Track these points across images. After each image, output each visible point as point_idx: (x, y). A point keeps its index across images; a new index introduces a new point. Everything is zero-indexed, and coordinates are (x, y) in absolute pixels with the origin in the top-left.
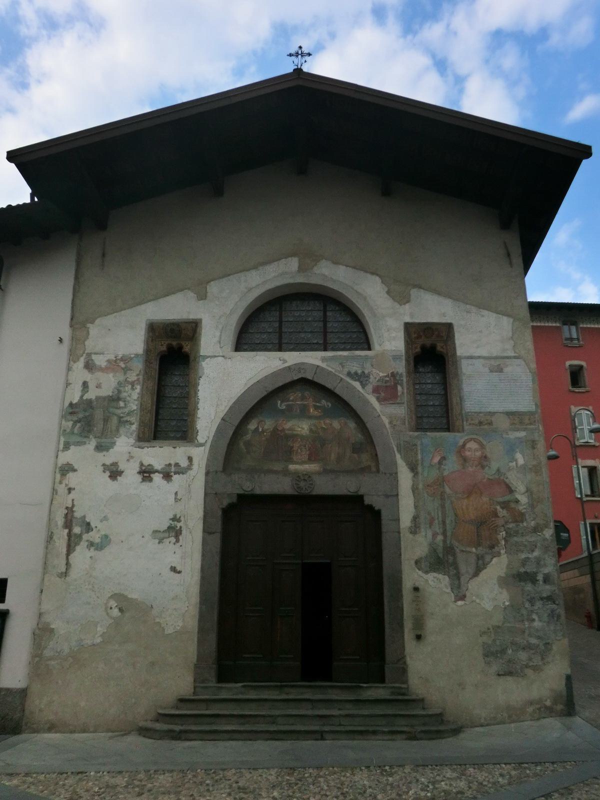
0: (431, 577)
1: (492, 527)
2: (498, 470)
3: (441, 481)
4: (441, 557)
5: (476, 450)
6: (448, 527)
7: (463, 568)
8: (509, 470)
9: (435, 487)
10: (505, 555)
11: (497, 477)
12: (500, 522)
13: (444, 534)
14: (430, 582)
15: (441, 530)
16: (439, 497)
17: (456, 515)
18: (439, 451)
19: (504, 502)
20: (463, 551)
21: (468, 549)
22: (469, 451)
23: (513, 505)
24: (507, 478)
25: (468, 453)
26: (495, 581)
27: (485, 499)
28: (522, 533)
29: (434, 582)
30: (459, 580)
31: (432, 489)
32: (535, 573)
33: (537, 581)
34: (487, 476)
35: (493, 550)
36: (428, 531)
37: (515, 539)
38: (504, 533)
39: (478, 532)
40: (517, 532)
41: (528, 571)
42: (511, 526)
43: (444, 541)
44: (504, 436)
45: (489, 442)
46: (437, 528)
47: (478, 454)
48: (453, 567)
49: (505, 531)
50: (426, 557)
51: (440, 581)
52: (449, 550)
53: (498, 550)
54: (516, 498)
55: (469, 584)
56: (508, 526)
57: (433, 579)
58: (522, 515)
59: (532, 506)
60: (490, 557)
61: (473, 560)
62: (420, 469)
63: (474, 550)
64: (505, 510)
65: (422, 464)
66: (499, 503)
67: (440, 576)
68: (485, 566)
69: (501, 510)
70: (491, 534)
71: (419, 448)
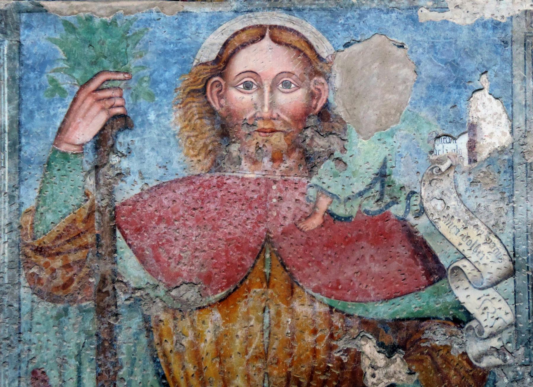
2: (382, 176)
3: (105, 225)
5: (282, 82)
8: (435, 171)
9: (72, 258)
11: (371, 206)
16: (89, 304)
19: (397, 324)
22: (248, 86)
23: (438, 336)
24: (422, 211)
25: (240, 99)
27: (309, 308)
31: (58, 263)
34: (324, 204)
45: (347, 45)
47: (292, 100)
54: (460, 306)
64: (398, 357)
66: (370, 326)
69: (381, 359)
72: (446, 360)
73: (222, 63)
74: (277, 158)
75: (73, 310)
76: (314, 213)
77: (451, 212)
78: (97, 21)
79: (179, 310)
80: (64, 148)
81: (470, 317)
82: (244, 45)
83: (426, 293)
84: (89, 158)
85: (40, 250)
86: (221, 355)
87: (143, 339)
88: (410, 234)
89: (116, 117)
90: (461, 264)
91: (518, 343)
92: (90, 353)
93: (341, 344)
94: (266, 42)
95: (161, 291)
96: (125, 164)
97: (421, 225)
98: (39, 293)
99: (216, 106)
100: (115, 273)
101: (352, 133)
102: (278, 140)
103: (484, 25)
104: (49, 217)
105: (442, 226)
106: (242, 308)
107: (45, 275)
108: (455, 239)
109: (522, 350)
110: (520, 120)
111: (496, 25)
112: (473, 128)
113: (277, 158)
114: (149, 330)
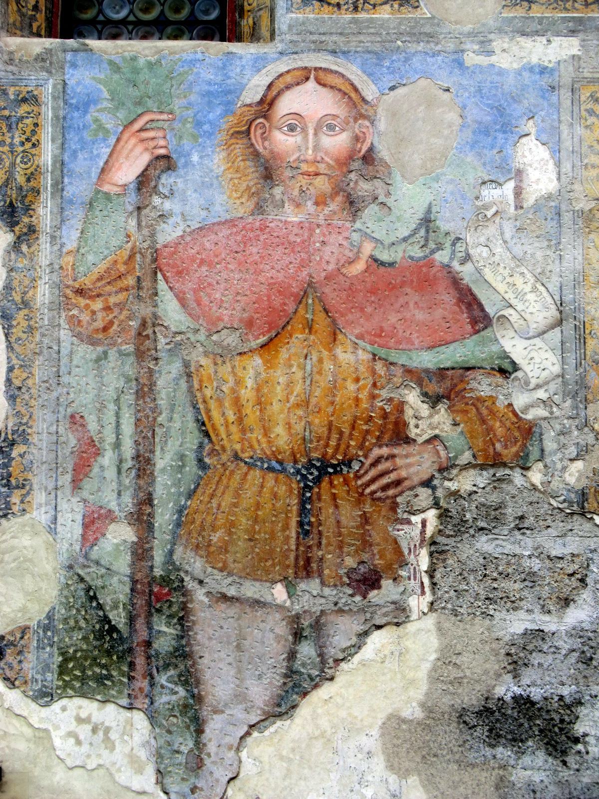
0: (69, 713)
1: (373, 487)
2: (427, 222)
4: (121, 626)
5: (326, 125)
6: (164, 487)
7: (219, 677)
8: (481, 217)
9: (112, 300)
10: (430, 621)
11: (416, 252)
12: (415, 464)
13: (142, 516)
14: (57, 742)
15: (128, 500)
16: (130, 348)
17: (204, 429)
18: (141, 130)
19: (441, 373)
20: (224, 598)
21: (251, 590)
22: (292, 128)
24: (467, 258)
25: (283, 141)
26: (372, 741)
27: (351, 356)
28: (522, 518)
29: (79, 742)
30: (200, 731)
31: (98, 305)
32: (568, 707)
33: (576, 741)
34: (368, 249)
35: (373, 594)
36: (63, 505)
37: (484, 544)
38: (431, 515)
39: (302, 511)
40: (494, 516)
41: (536, 694)
42: (465, 482)
43: (141, 552)
44: (471, 59)
45: (392, 88)
46: (110, 490)
47: (336, 142)
48: (172, 672)
49: (436, 505)
50: (48, 625)
51: (107, 738)
52: (161, 593)
53: (396, 597)
54: (505, 356)
55: (244, 754)
56: (453, 486)
57: (73, 726)
58: (528, 431)
59: (578, 391)
60: (355, 625)
61: (269, 638)
62: (45, 212)
63: (279, 593)
64: (442, 407)
65: (59, 187)
66: (416, 376)
67: (111, 714)
68: (324, 674)
69: (424, 409)
70: (365, 519)
71: (48, 112)
72: (492, 412)
73: (266, 105)
74: (320, 202)
75: (112, 353)
76: (357, 258)
77: (497, 259)
78: (142, 62)
79: (220, 355)
80: (106, 188)
81: (515, 367)
82: (288, 87)
83: (471, 342)
84: (132, 198)
85: (80, 292)
86: (261, 403)
87: (183, 385)
88: (456, 282)
89: (158, 158)
90: (507, 312)
91: (565, 395)
92: (129, 398)
93: (384, 393)
94: (311, 84)
95: (202, 336)
96: (167, 205)
97: (466, 272)
98: (78, 336)
99: (260, 148)
100: (155, 316)
101: (397, 177)
102: (322, 184)
103: (531, 69)
104: (90, 258)
105: (488, 274)
106: (284, 354)
107: (85, 317)
108: (501, 287)
109: (569, 402)
110: (567, 167)
111: (543, 70)
112: (519, 174)
113: (320, 202)
114: (189, 375)
